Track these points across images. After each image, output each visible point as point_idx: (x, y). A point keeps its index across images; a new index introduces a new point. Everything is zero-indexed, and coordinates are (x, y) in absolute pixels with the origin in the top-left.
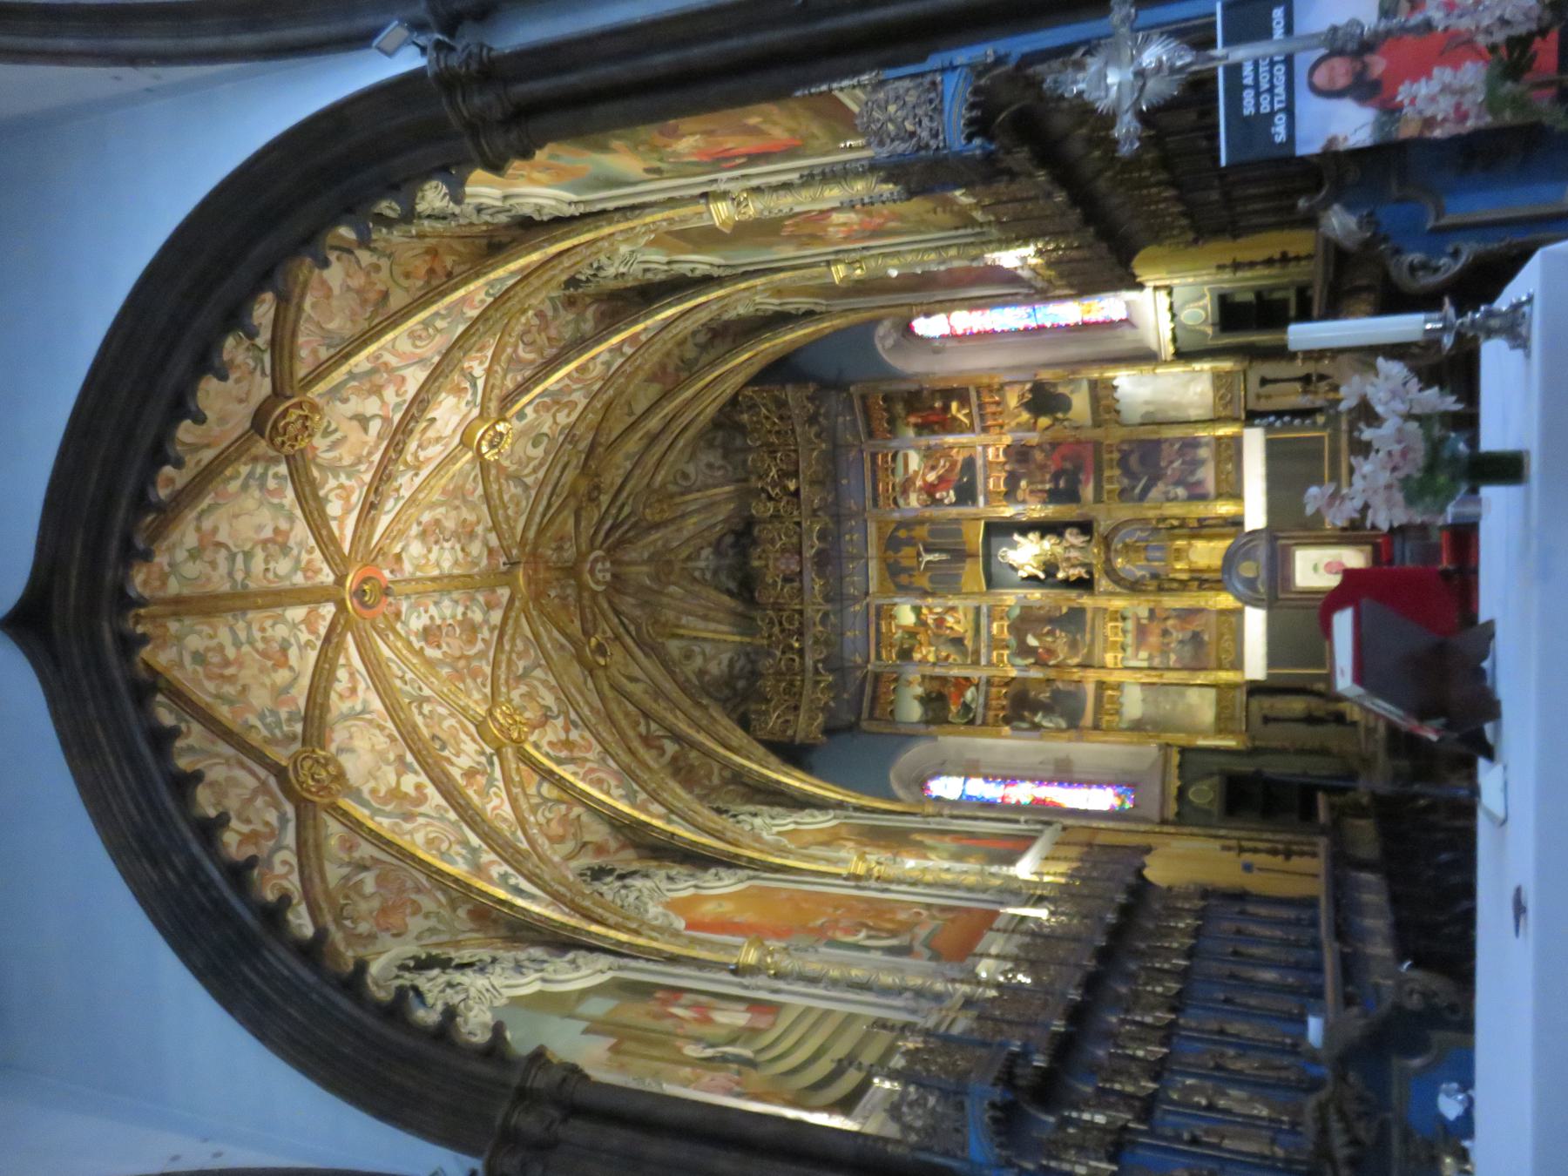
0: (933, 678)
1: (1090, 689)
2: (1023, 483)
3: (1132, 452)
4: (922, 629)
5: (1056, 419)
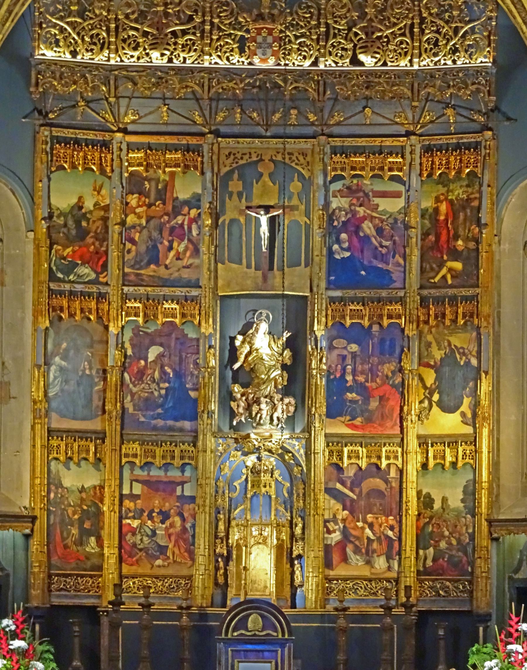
0: (105, 219)
1: (95, 425)
2: (354, 347)
3: (387, 481)
4: (170, 208)
5: (431, 394)
